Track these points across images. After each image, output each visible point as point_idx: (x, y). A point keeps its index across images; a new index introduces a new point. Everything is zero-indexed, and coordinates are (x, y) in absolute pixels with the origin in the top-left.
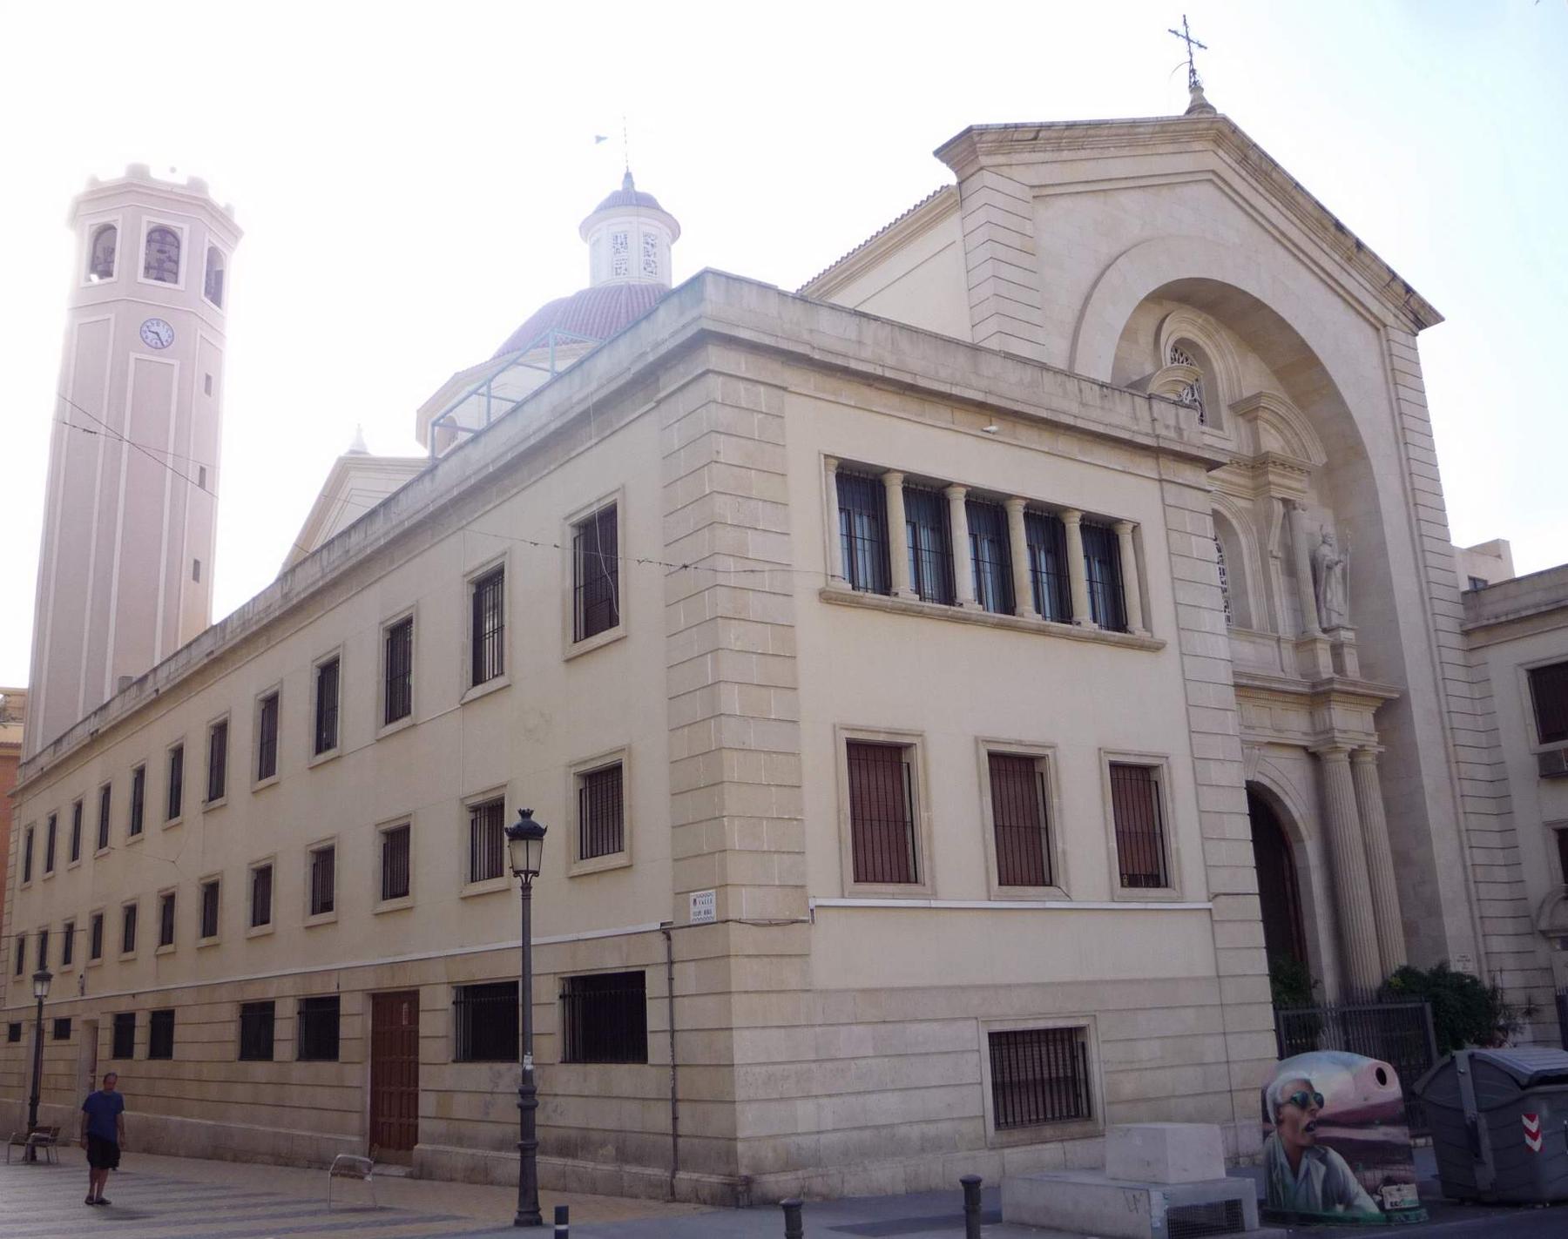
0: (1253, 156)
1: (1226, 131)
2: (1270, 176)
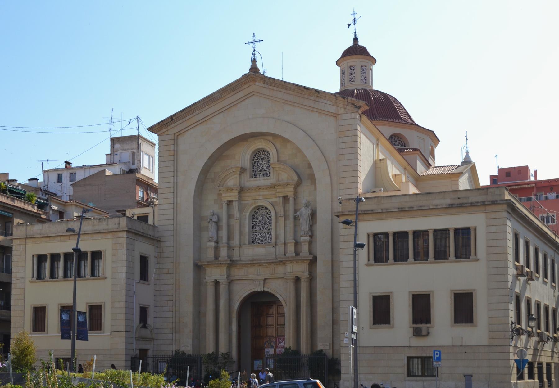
2: (275, 83)
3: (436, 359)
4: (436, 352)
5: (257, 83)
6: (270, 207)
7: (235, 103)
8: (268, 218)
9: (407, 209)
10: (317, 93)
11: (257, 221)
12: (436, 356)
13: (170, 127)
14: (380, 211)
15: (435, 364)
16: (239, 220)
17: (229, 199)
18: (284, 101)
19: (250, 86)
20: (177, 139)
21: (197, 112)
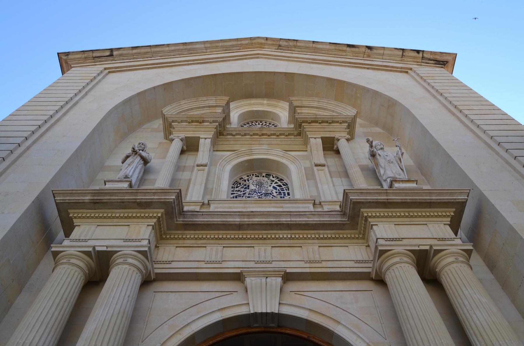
0: (282, 43)
1: (263, 41)
8: (274, 187)
10: (369, 51)
11: (244, 191)
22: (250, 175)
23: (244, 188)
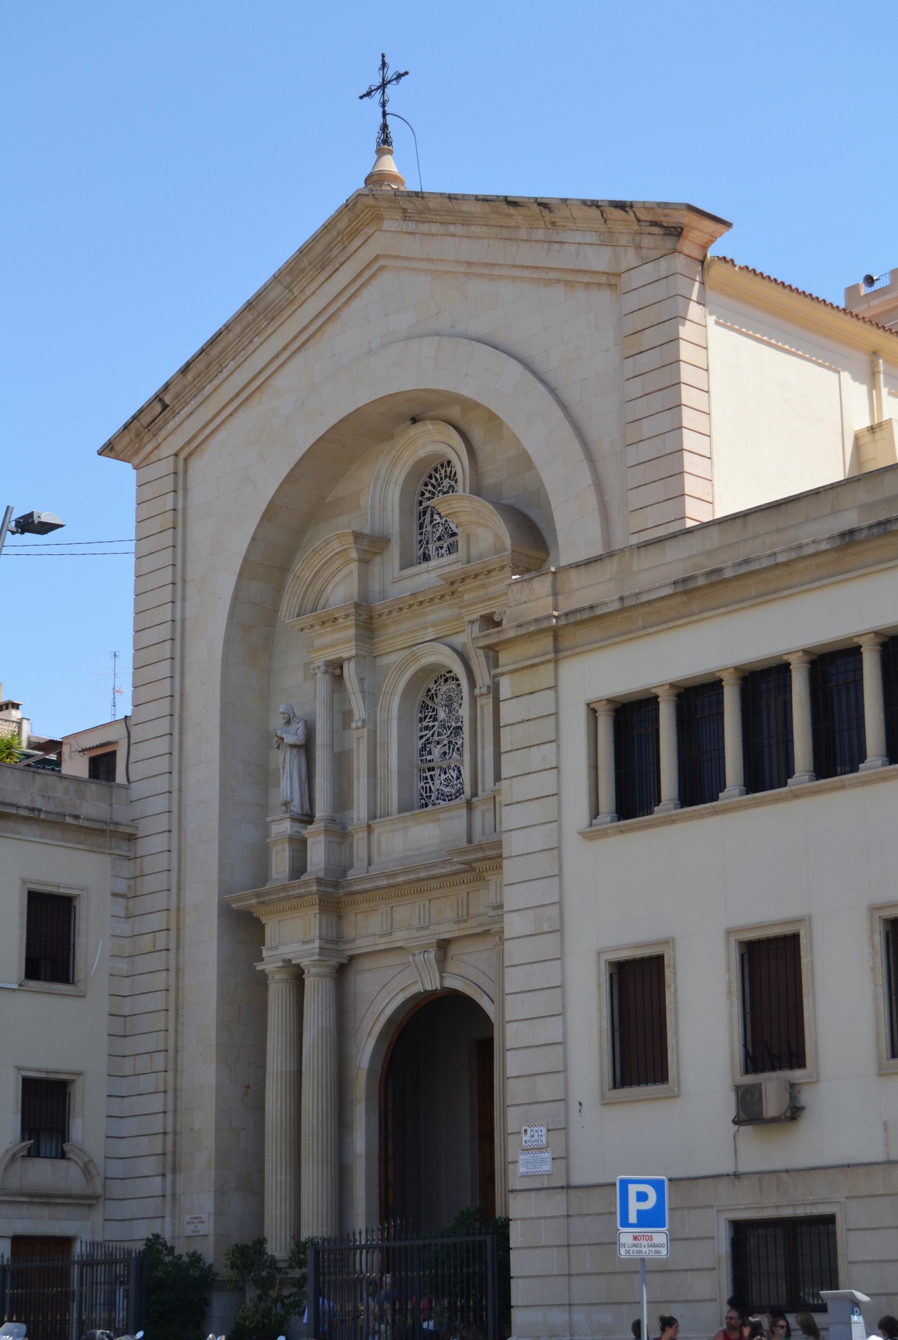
2: (429, 210)
3: (633, 1219)
4: (633, 1189)
5: (387, 225)
6: (459, 670)
7: (331, 310)
9: (701, 582)
10: (546, 212)
11: (433, 726)
12: (634, 1206)
13: (164, 433)
14: (616, 606)
15: (631, 1241)
16: (366, 729)
17: (331, 655)
18: (462, 269)
19: (369, 238)
20: (185, 471)
21: (232, 365)
22: (438, 678)
23: (431, 720)
